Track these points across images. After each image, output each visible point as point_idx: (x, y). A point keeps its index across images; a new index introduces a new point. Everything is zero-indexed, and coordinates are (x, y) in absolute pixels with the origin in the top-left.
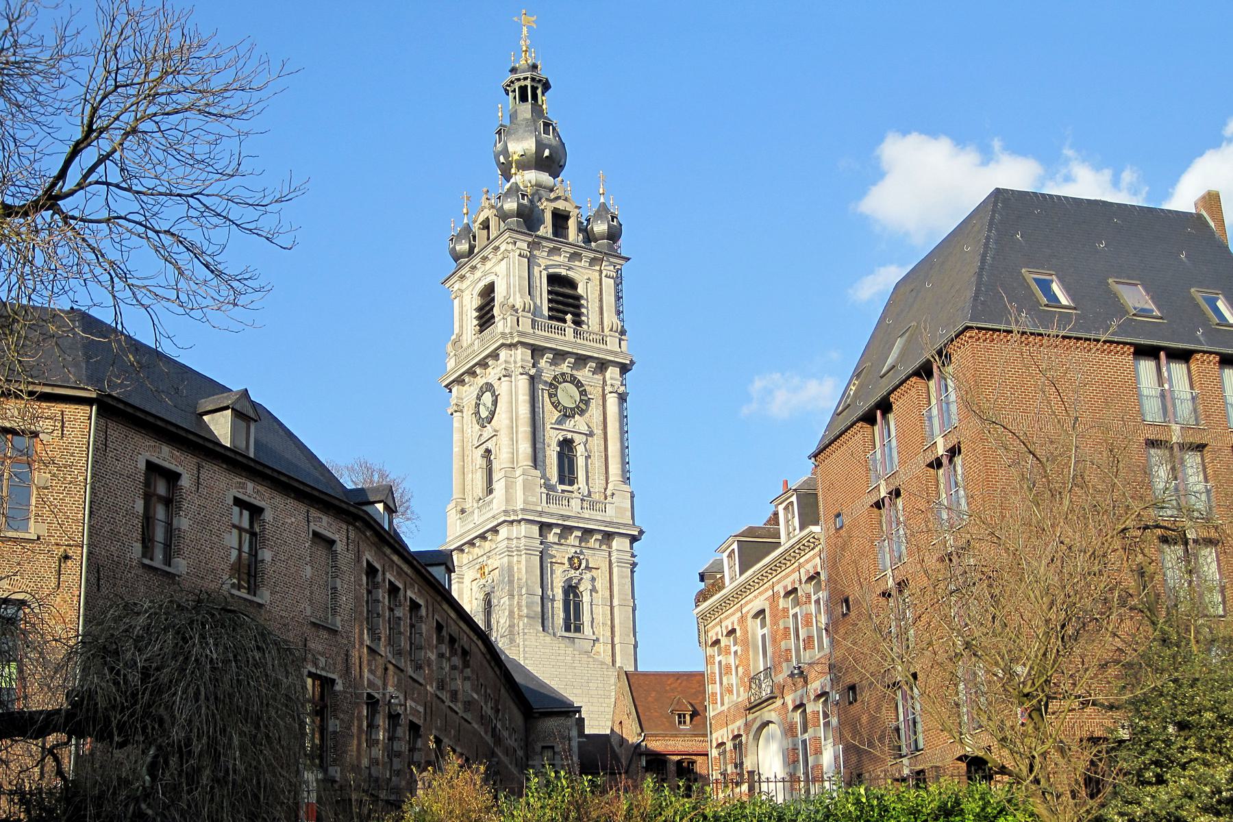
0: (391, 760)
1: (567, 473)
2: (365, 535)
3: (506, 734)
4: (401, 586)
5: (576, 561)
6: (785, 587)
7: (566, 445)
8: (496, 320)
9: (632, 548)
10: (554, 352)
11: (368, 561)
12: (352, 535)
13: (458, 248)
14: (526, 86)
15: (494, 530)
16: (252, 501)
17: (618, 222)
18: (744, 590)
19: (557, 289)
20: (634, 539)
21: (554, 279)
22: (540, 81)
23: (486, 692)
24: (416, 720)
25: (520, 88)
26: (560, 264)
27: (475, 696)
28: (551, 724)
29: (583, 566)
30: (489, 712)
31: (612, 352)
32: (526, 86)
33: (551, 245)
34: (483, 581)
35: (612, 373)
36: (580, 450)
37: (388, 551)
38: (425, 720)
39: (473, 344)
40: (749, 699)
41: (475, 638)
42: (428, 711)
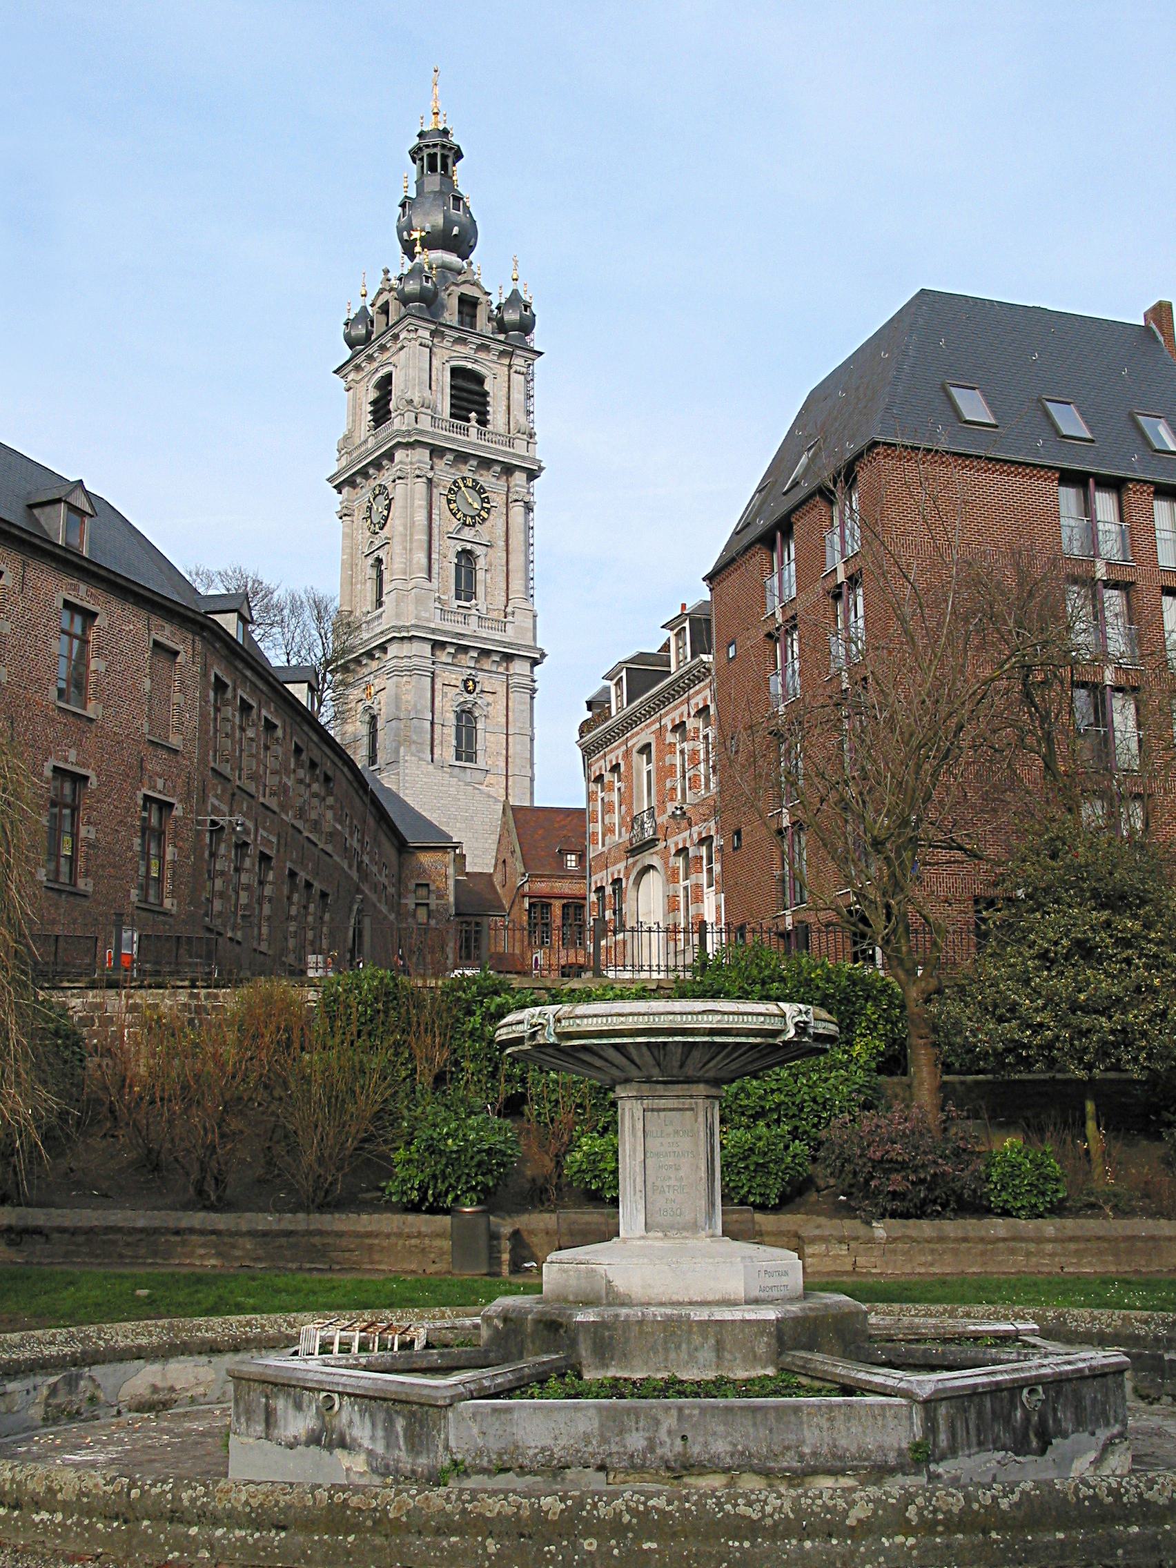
0: (238, 893)
1: (466, 588)
2: (214, 647)
3: (375, 869)
4: (254, 704)
5: (471, 683)
6: (673, 720)
7: (466, 556)
8: (393, 415)
9: (532, 672)
11: (216, 676)
12: (199, 645)
13: (353, 333)
14: (436, 154)
15: (383, 648)
16: (85, 604)
17: (531, 312)
18: (630, 723)
20: (535, 662)
21: (455, 372)
22: (451, 149)
23: (351, 823)
24: (267, 851)
25: (429, 155)
26: (465, 356)
27: (339, 827)
28: (426, 859)
29: (478, 690)
30: (355, 844)
31: (519, 456)
32: (436, 154)
33: (457, 335)
34: (368, 703)
35: (520, 477)
36: (481, 563)
37: (240, 666)
38: (278, 851)
39: (366, 441)
40: (631, 840)
41: (340, 764)
42: (282, 841)
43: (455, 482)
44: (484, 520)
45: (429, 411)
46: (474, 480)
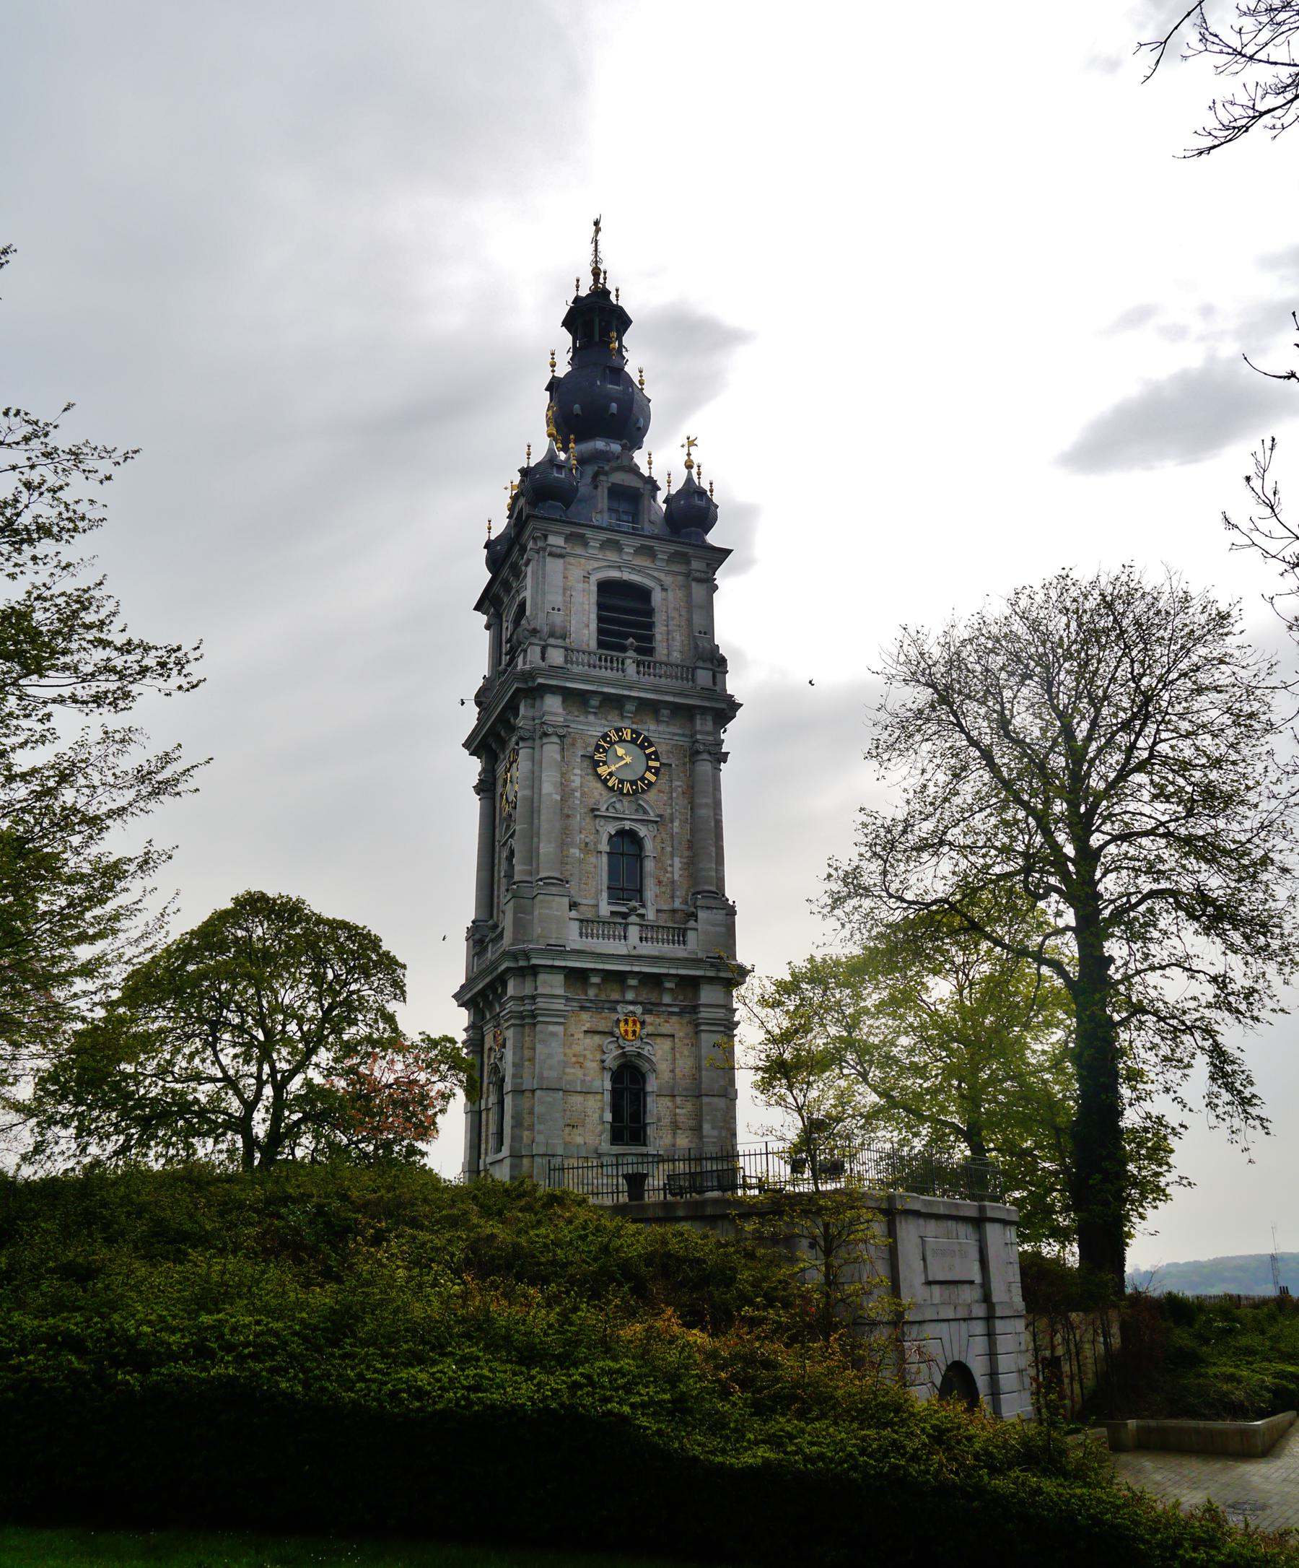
19: (616, 601)
21: (606, 588)
36: (649, 845)
43: (604, 737)
44: (650, 784)
45: (559, 642)
46: (633, 731)
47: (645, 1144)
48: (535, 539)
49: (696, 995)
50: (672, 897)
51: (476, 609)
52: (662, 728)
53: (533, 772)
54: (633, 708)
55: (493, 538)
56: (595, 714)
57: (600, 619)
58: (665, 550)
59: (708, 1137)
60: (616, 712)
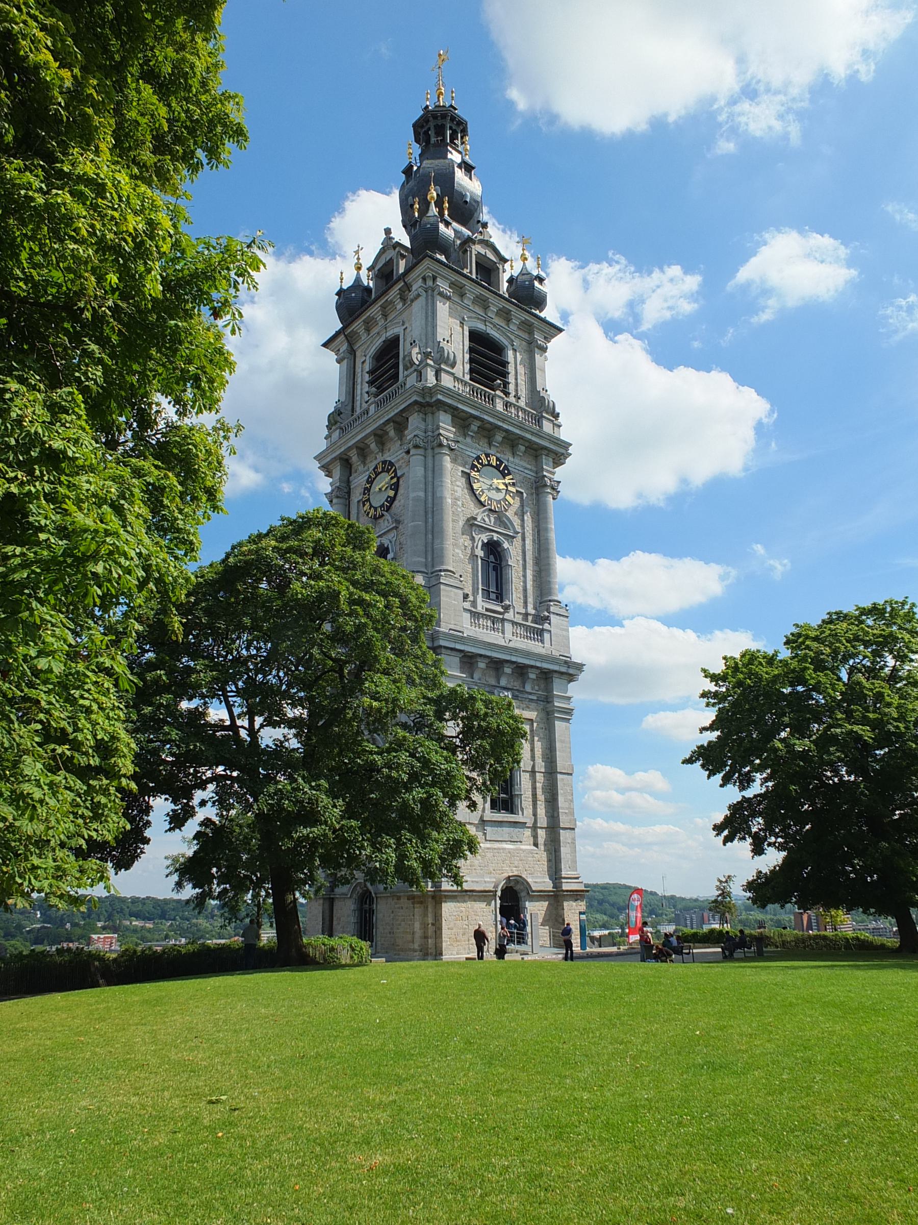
10: (478, 423)
21: (476, 337)
43: (478, 458)
46: (498, 459)
47: (512, 813)
48: (424, 279)
49: (549, 689)
50: (526, 603)
51: (325, 345)
52: (517, 460)
53: (425, 477)
54: (500, 439)
55: (345, 287)
56: (472, 437)
57: (471, 361)
58: (518, 315)
59: (563, 808)
60: (486, 440)
